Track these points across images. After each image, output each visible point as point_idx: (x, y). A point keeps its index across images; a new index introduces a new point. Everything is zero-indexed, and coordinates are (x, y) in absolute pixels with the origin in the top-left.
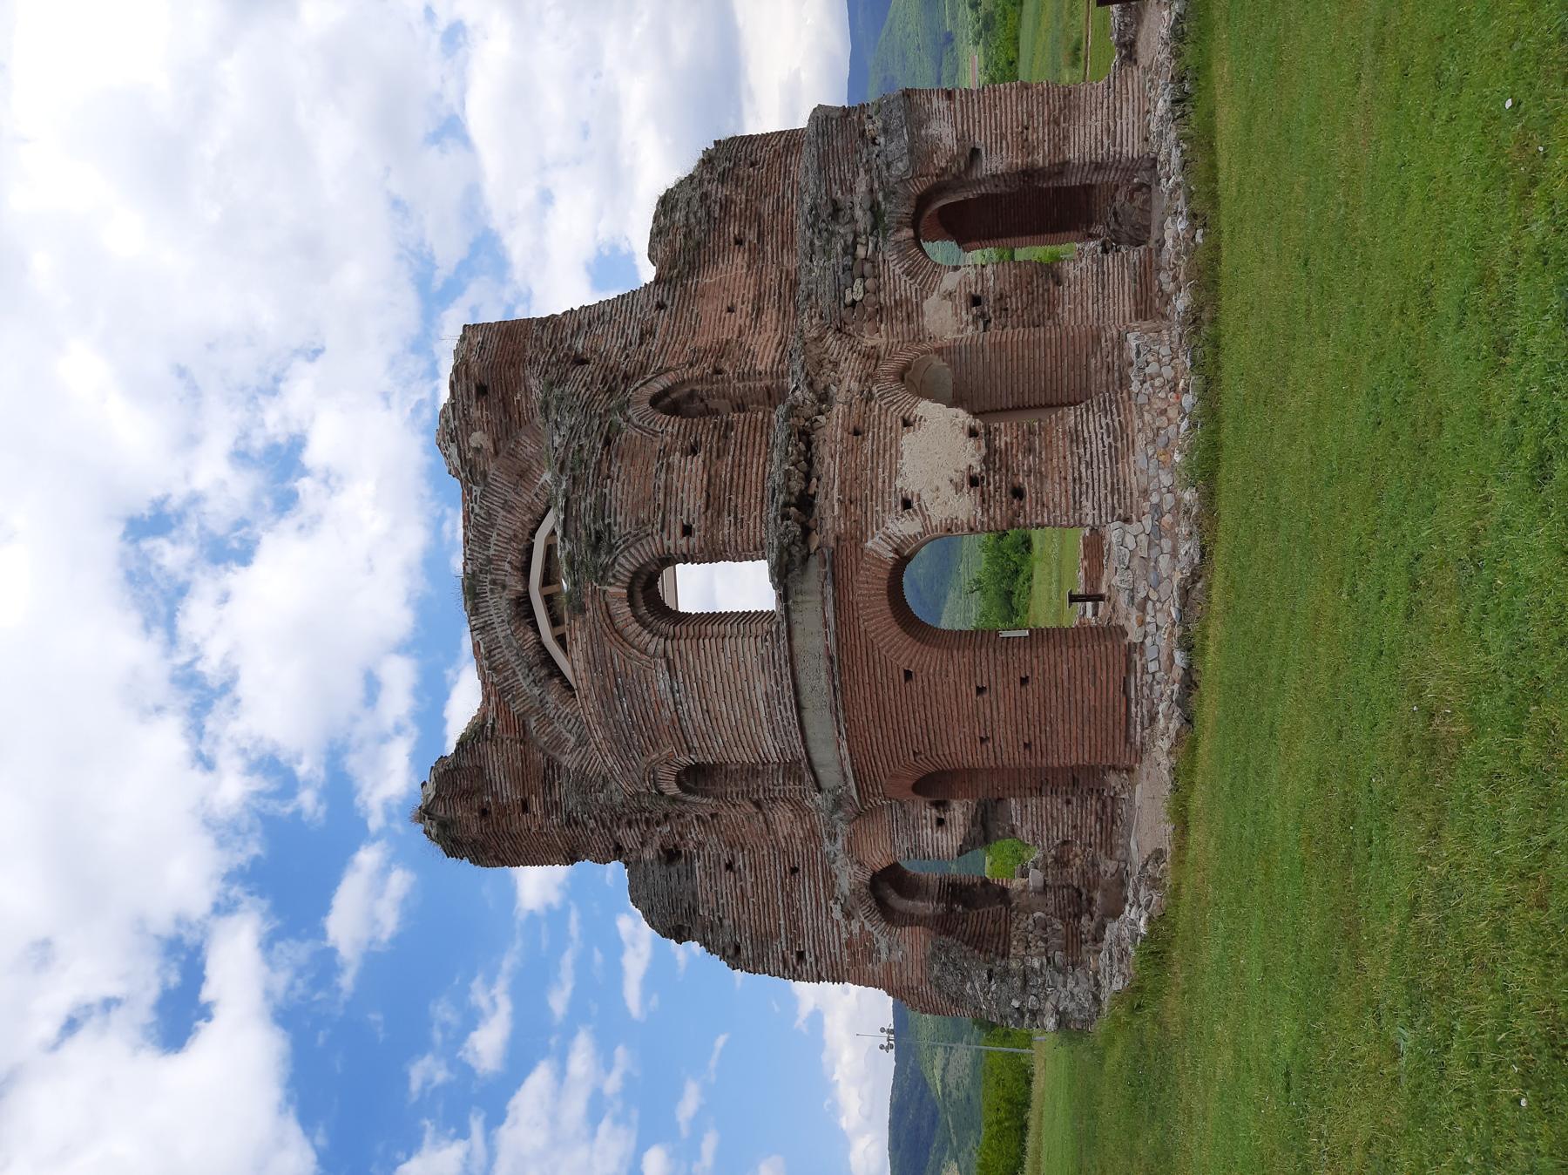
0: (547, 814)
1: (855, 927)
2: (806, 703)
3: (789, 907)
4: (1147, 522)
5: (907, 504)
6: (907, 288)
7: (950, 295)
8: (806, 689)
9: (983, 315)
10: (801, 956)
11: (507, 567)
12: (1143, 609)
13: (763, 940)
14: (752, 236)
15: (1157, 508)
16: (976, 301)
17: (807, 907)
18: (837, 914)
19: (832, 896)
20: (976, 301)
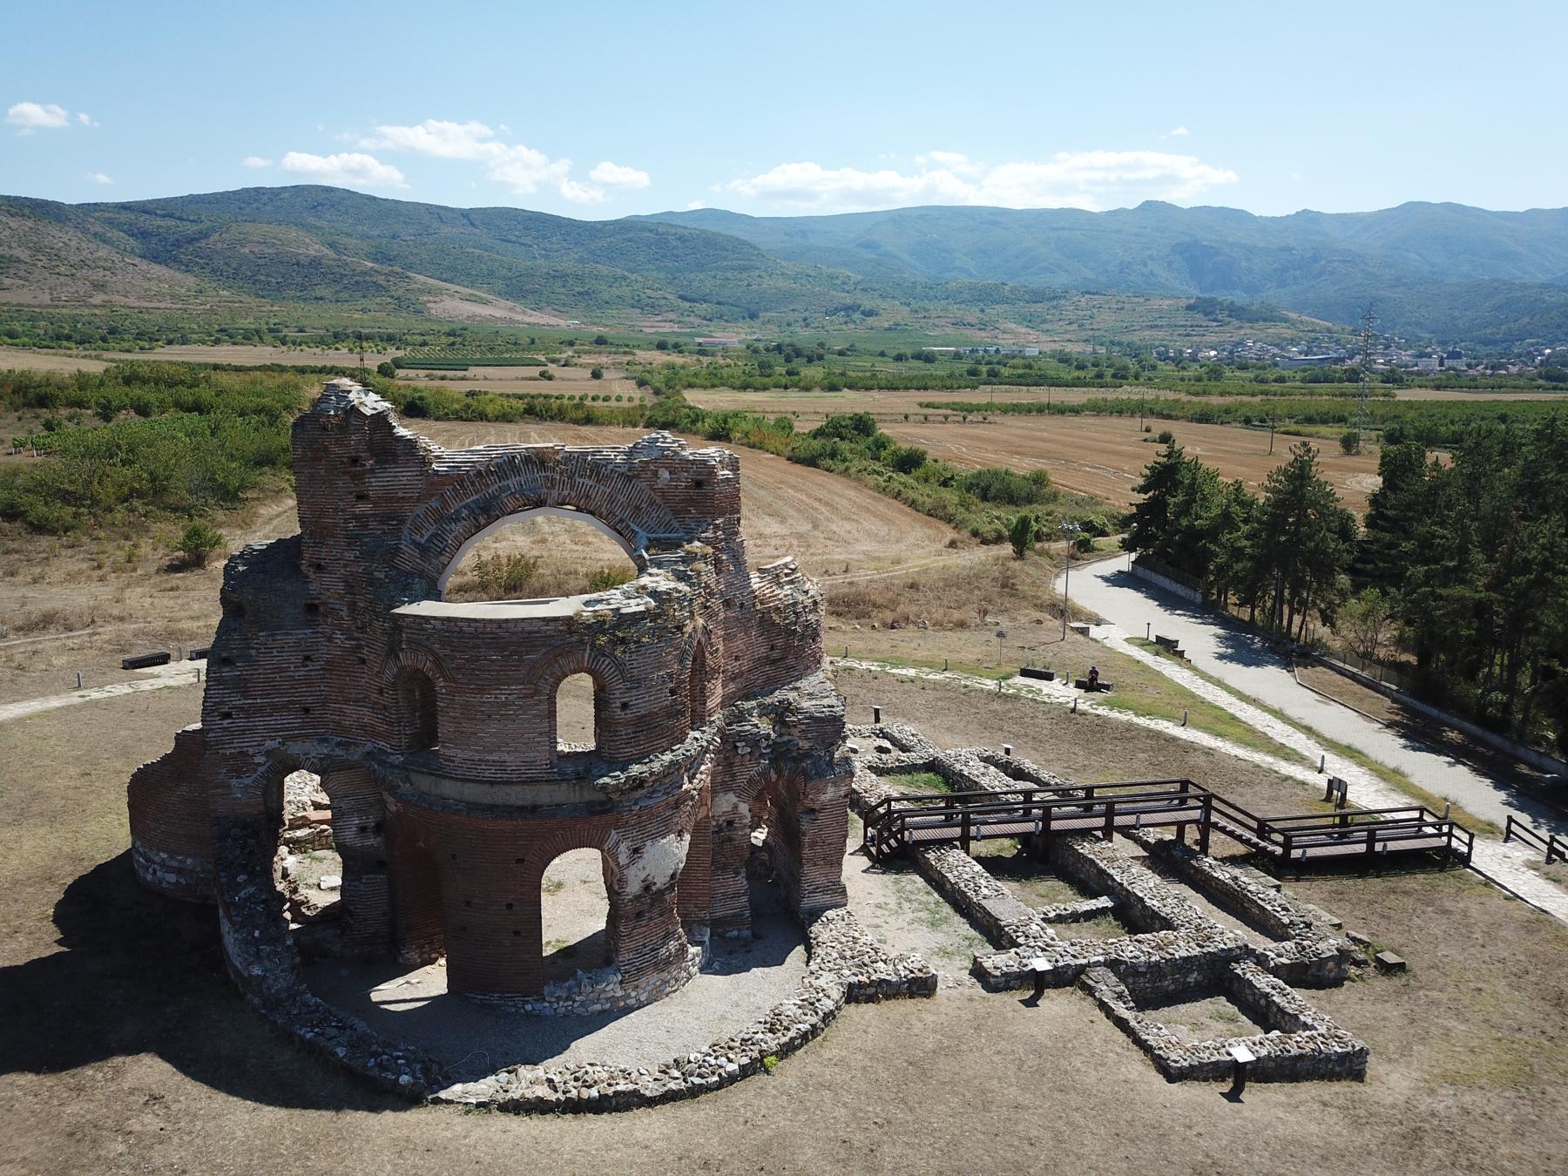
0: (356, 517)
1: (260, 759)
2: (496, 788)
3: (275, 708)
4: (620, 993)
5: (636, 851)
6: (742, 780)
7: (736, 807)
8: (508, 789)
9: (721, 830)
10: (227, 715)
11: (566, 492)
12: (567, 999)
13: (242, 686)
14: (776, 654)
15: (629, 996)
16: (730, 823)
17: (275, 721)
18: (269, 744)
19: (285, 739)
20: (730, 823)
